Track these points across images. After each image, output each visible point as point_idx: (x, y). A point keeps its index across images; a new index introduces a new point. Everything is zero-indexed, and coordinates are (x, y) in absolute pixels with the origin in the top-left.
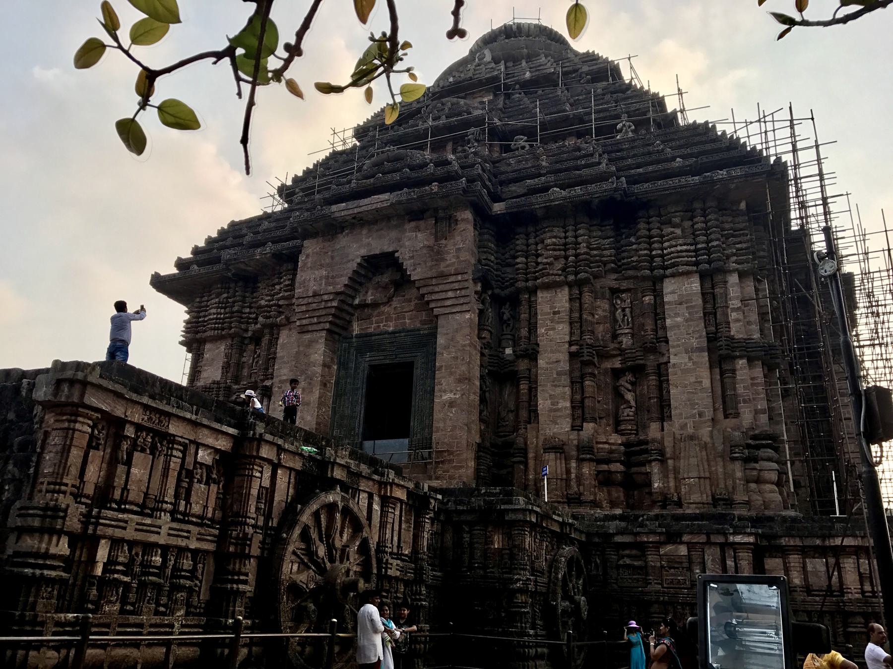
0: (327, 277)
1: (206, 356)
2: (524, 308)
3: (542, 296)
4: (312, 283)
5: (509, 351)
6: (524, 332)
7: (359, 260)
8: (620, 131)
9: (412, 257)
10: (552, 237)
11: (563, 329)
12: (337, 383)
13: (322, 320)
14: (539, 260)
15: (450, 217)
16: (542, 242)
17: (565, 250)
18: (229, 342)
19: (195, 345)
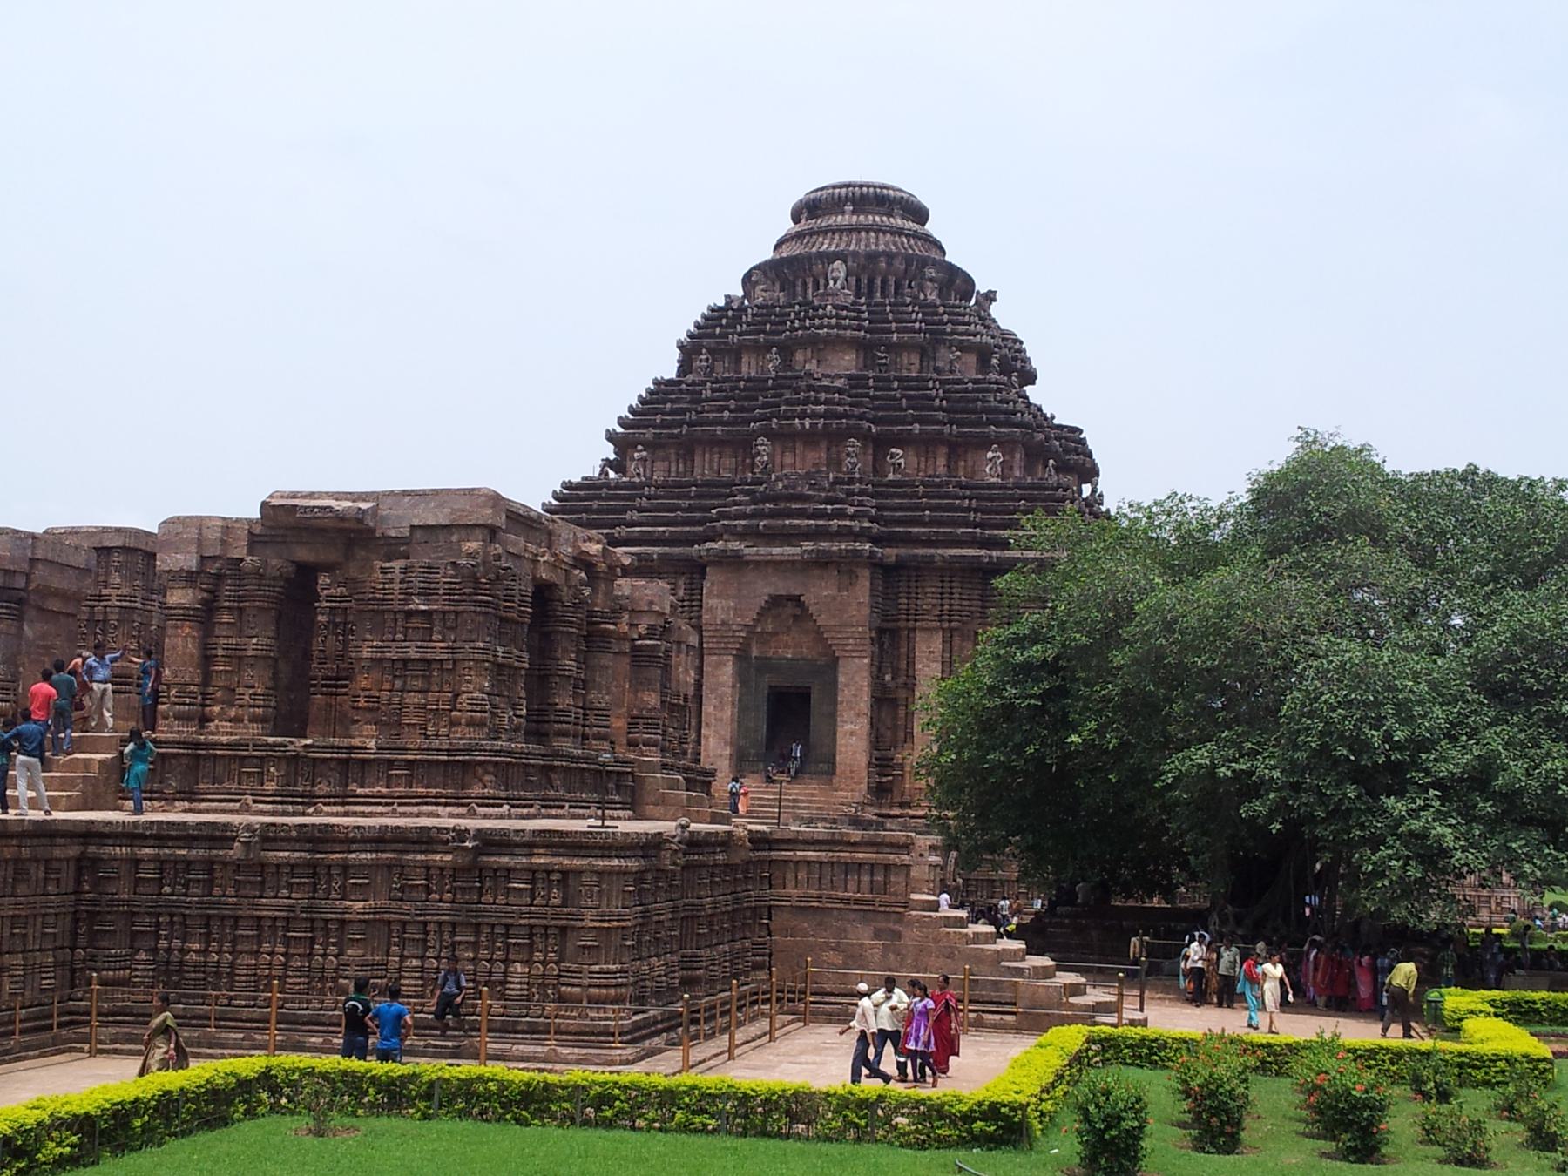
2: (904, 643)
3: (919, 636)
4: (719, 611)
5: (888, 678)
6: (903, 665)
7: (766, 598)
8: (991, 460)
9: (816, 604)
10: (931, 587)
11: (937, 666)
12: (740, 700)
13: (730, 646)
14: (919, 602)
15: (851, 571)
16: (923, 588)
17: (942, 599)
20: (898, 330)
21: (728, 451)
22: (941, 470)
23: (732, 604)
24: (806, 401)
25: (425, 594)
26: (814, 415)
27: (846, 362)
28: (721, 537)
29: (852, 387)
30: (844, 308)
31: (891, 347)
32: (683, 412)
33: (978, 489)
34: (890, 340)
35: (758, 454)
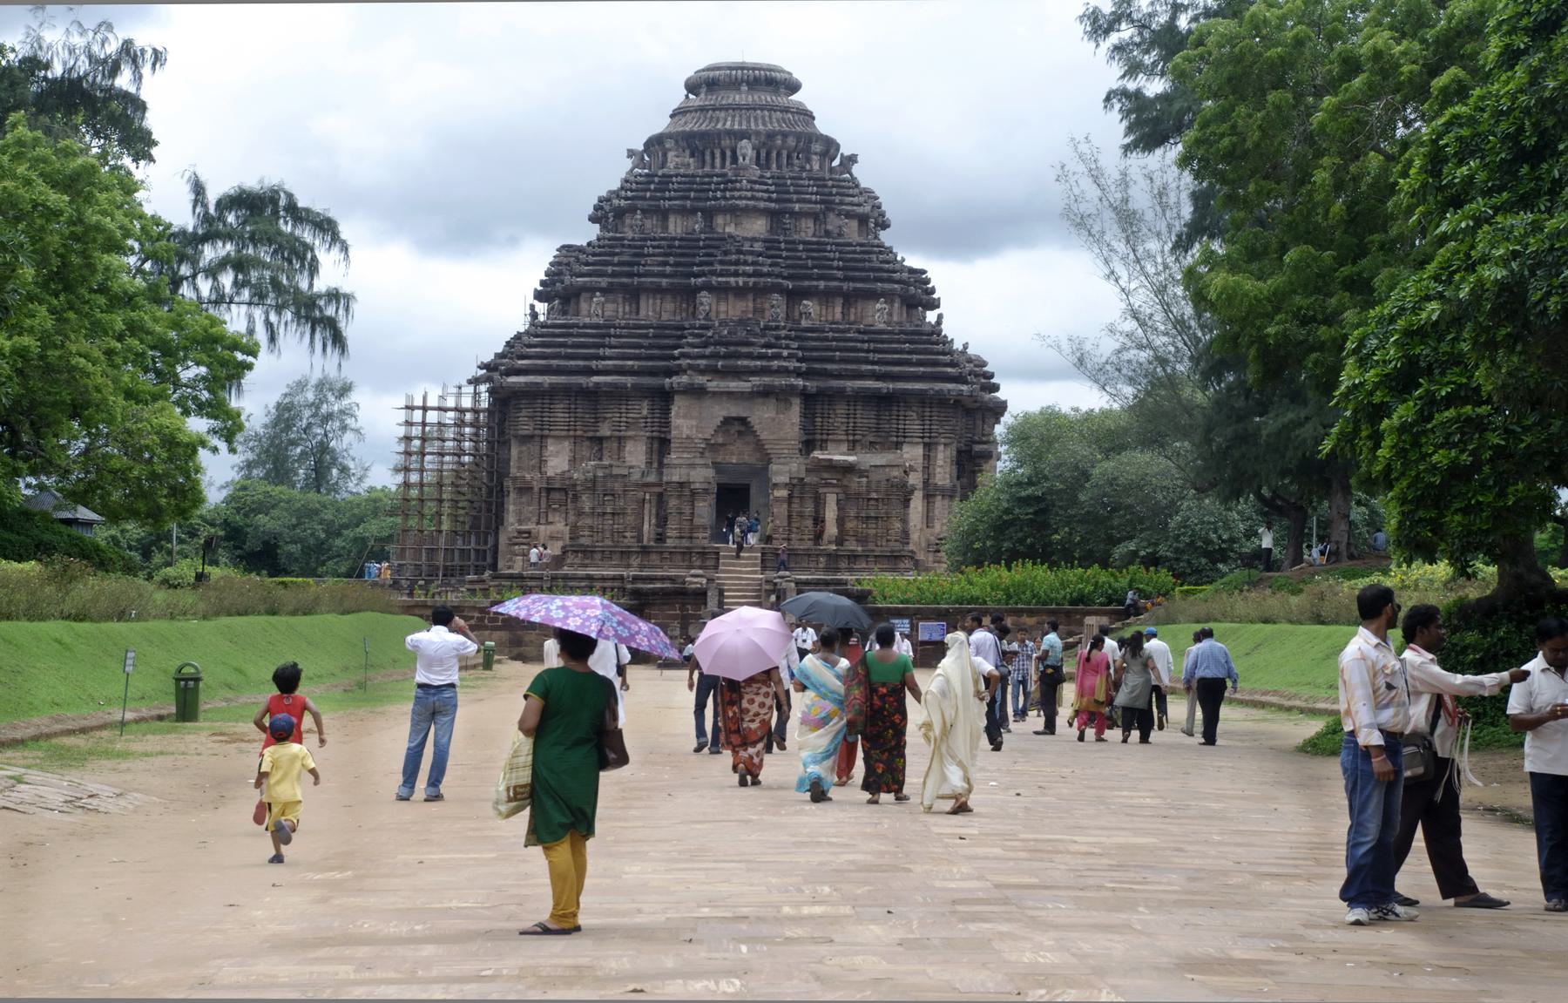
0: (697, 427)
1: (550, 448)
10: (841, 409)
18: (572, 440)
19: (537, 439)
20: (798, 201)
21: (669, 297)
22: (838, 316)
23: (694, 423)
24: (737, 263)
25: (876, 491)
26: (745, 274)
27: (758, 227)
28: (685, 372)
29: (768, 249)
30: (755, 182)
31: (792, 213)
32: (631, 264)
33: (871, 334)
34: (793, 208)
35: (702, 304)
